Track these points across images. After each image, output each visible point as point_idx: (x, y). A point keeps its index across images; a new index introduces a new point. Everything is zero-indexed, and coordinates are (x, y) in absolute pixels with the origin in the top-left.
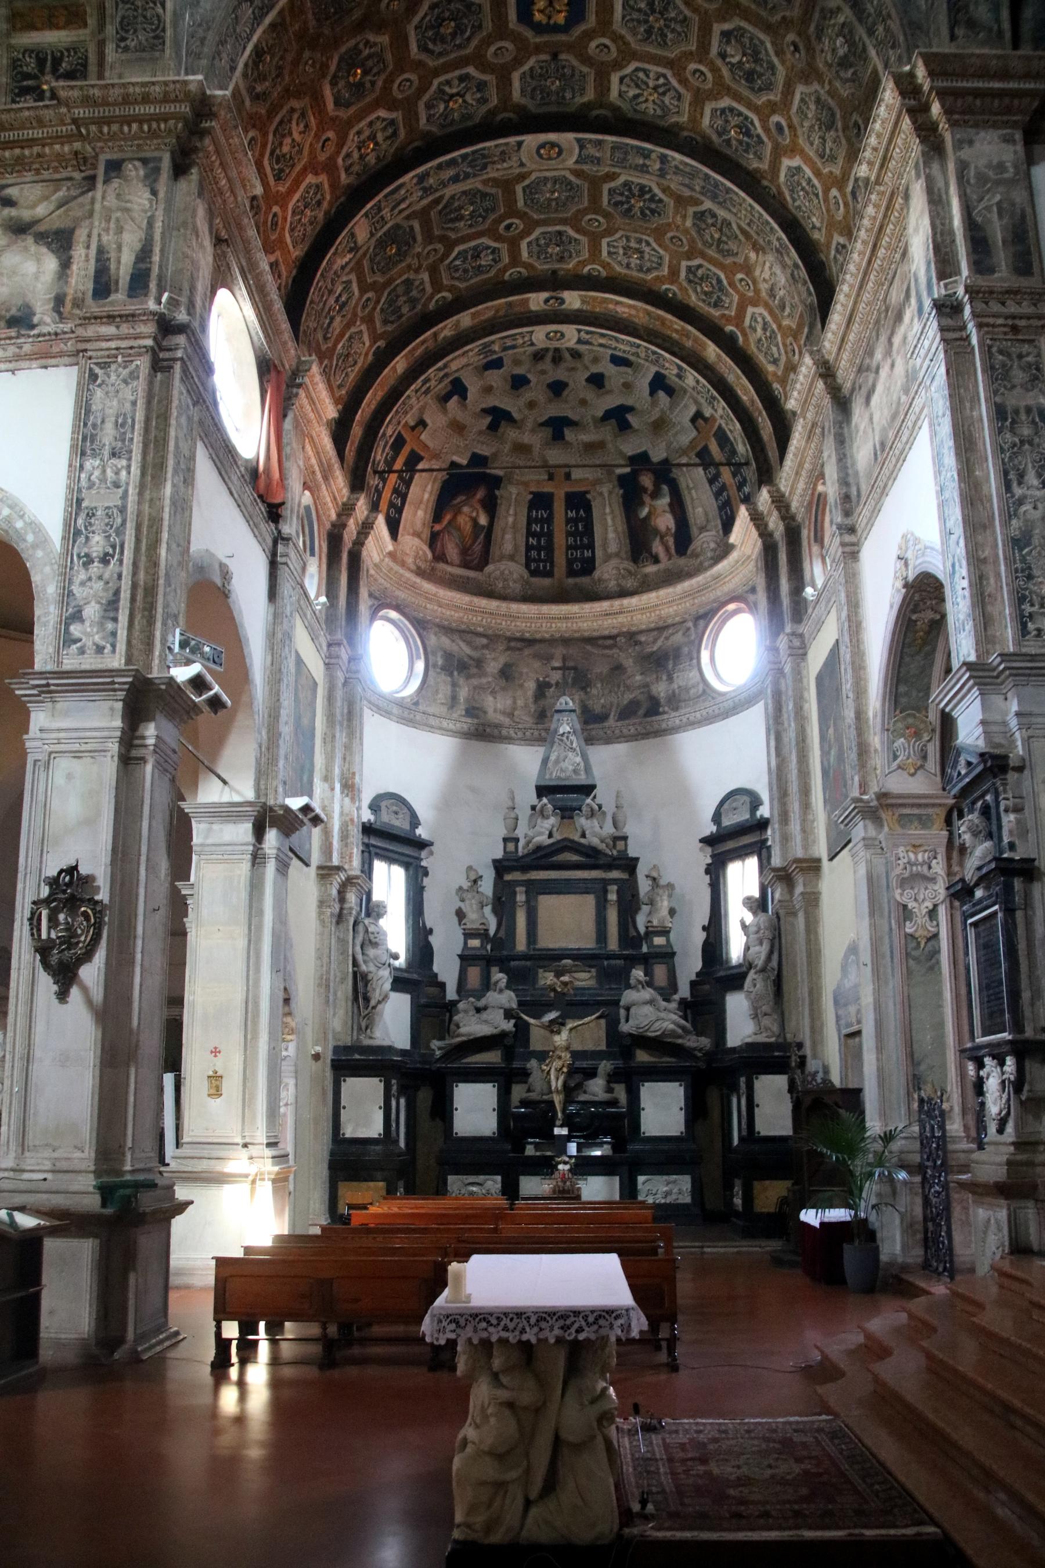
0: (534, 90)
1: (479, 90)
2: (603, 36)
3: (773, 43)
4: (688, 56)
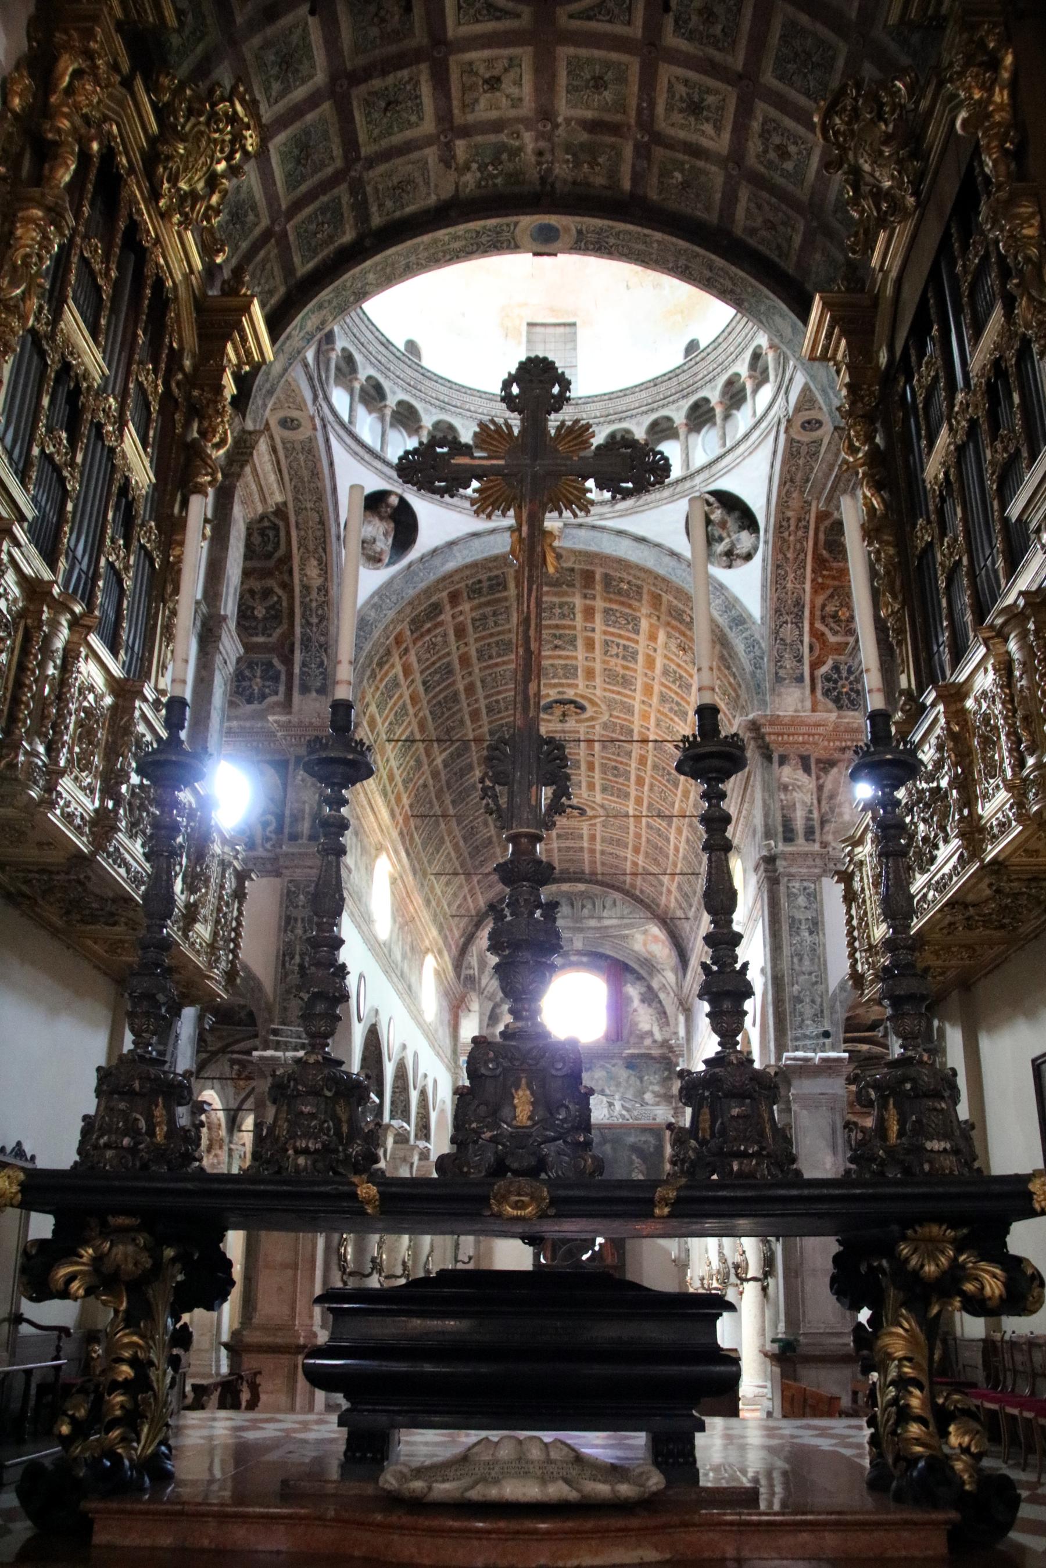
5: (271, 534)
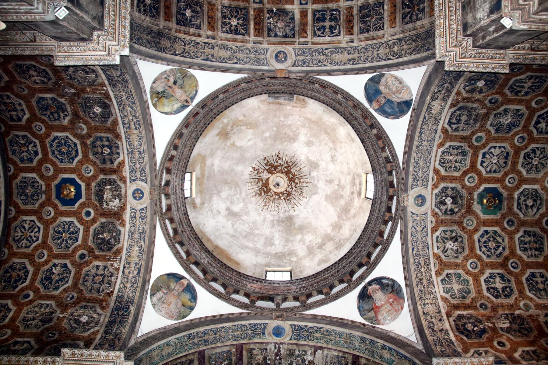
0: (26, 182)
1: (28, 159)
2: (55, 213)
4: (50, 249)
5: (454, 120)
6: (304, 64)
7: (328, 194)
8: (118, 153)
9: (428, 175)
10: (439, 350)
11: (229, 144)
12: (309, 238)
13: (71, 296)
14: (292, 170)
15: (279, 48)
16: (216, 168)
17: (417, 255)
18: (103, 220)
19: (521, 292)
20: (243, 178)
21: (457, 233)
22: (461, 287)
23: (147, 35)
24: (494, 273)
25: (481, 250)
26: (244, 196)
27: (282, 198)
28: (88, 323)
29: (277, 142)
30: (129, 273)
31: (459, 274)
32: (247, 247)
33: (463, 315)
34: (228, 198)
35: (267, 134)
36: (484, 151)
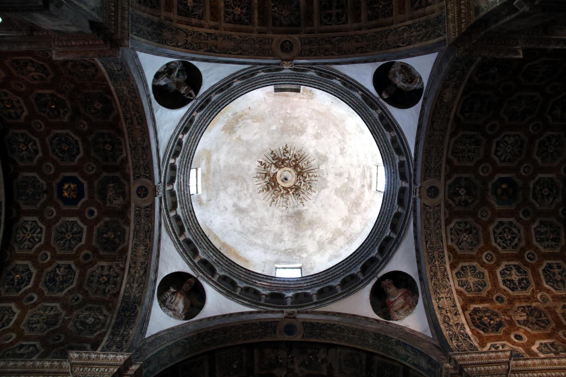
3: (73, 289)
4: (53, 251)
6: (311, 53)
7: (338, 187)
8: (121, 150)
9: (441, 165)
10: (455, 344)
11: (234, 138)
12: (319, 233)
13: (76, 298)
14: (300, 164)
15: (285, 37)
16: (222, 163)
17: (431, 248)
18: (107, 219)
19: (538, 284)
20: (250, 172)
21: (471, 225)
22: (476, 280)
23: (148, 27)
24: (510, 265)
25: (496, 242)
26: (251, 191)
27: (291, 193)
28: (94, 325)
29: (284, 136)
30: (135, 273)
31: (474, 267)
32: (255, 244)
33: (479, 308)
34: (234, 194)
35: (274, 127)
36: (498, 139)
